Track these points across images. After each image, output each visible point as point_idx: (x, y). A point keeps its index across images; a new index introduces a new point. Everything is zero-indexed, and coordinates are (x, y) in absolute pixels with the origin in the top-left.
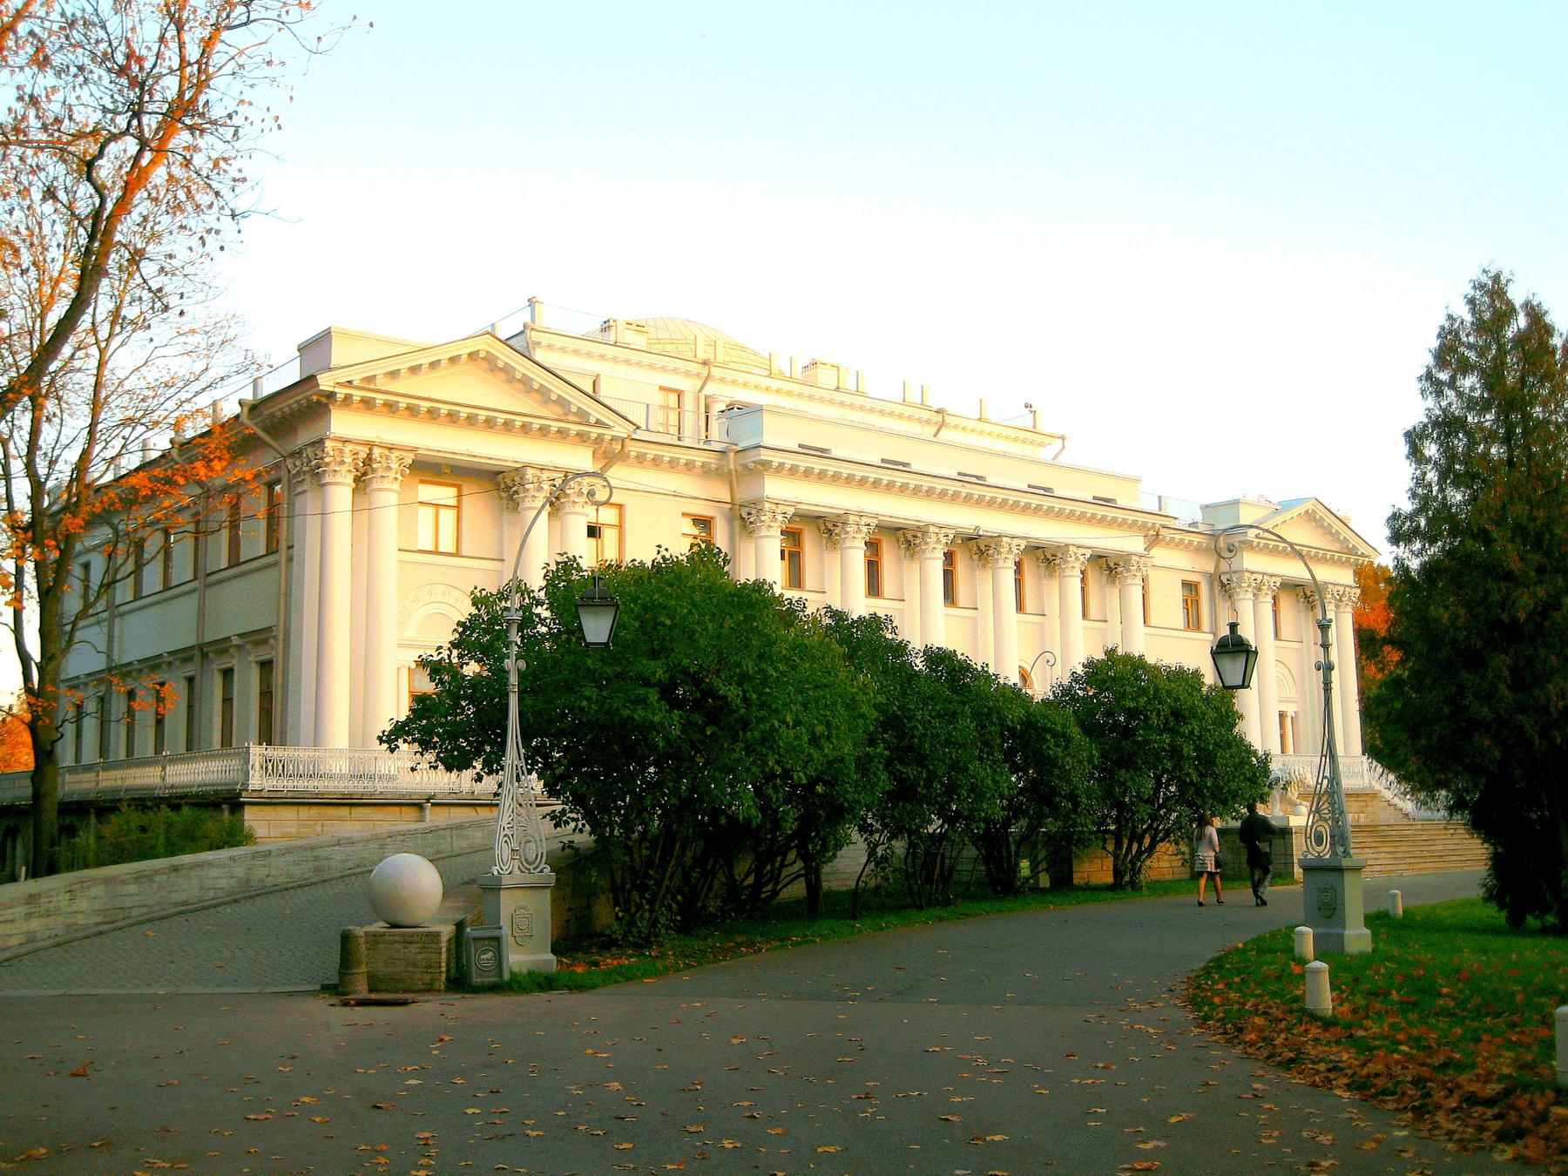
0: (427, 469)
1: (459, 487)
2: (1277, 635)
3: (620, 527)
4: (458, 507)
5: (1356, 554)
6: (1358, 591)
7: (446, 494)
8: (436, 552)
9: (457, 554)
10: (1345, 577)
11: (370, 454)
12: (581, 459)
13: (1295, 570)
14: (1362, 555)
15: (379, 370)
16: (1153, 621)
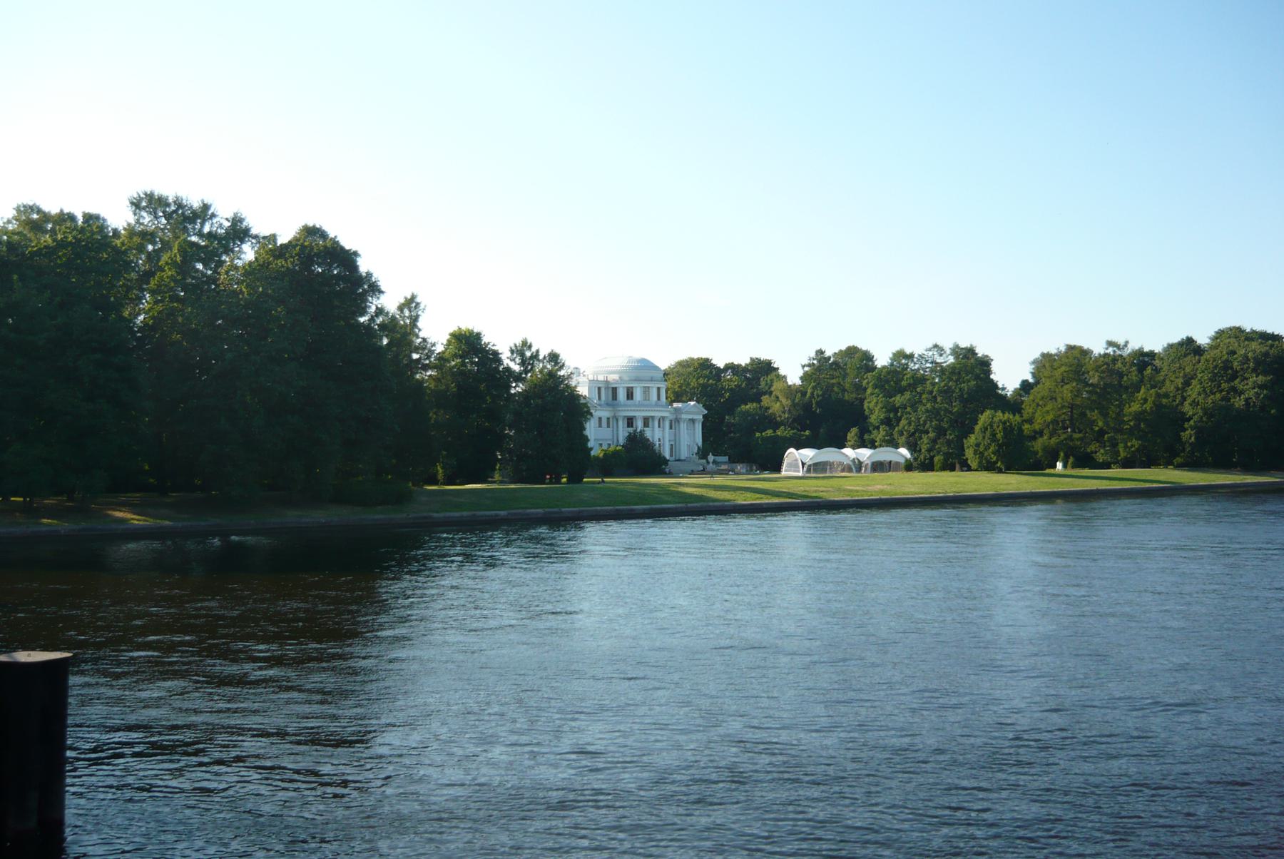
10: (701, 417)
13: (691, 417)
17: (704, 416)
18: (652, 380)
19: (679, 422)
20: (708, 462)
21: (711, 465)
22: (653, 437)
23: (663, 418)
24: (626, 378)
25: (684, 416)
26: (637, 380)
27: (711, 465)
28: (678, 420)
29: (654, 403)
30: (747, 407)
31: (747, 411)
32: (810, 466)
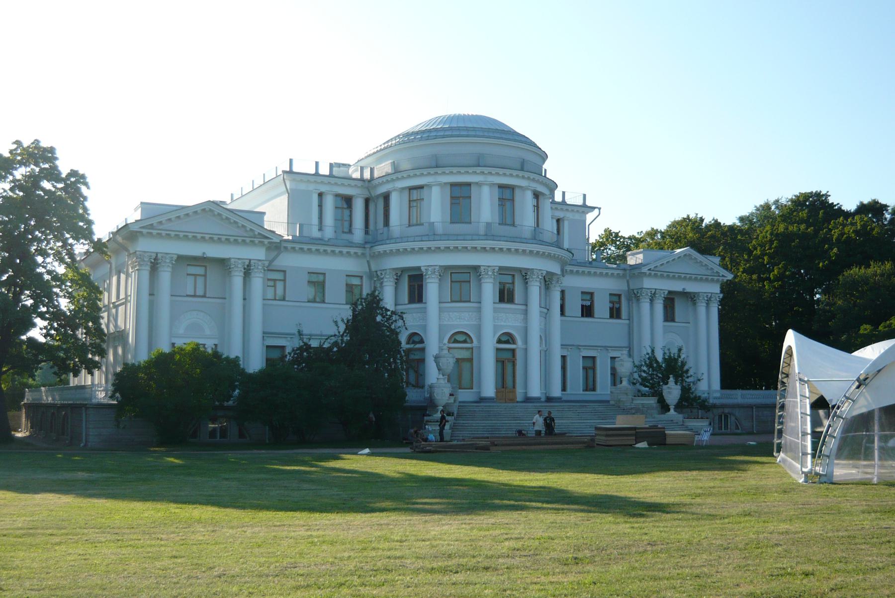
0: (183, 260)
1: (206, 267)
2: (562, 313)
3: (284, 280)
4: (205, 276)
5: (719, 276)
6: (721, 296)
7: (200, 271)
8: (195, 296)
9: (204, 296)
10: (716, 289)
11: (157, 256)
12: (258, 254)
14: (723, 276)
15: (163, 219)
16: (567, 312)
17: (728, 289)
18: (479, 163)
19: (638, 300)
20: (665, 408)
21: (672, 411)
22: (479, 328)
23: (525, 275)
24: (405, 166)
25: (649, 284)
26: (436, 164)
27: (672, 411)
28: (634, 296)
29: (482, 231)
30: (870, 271)
31: (865, 280)
32: (863, 421)
